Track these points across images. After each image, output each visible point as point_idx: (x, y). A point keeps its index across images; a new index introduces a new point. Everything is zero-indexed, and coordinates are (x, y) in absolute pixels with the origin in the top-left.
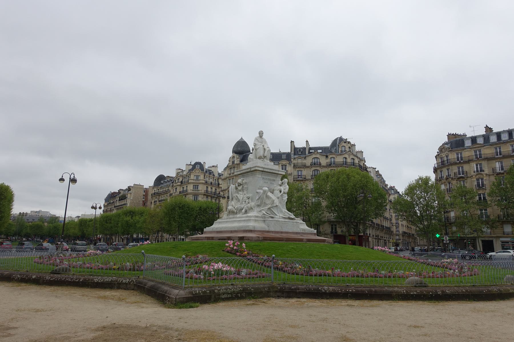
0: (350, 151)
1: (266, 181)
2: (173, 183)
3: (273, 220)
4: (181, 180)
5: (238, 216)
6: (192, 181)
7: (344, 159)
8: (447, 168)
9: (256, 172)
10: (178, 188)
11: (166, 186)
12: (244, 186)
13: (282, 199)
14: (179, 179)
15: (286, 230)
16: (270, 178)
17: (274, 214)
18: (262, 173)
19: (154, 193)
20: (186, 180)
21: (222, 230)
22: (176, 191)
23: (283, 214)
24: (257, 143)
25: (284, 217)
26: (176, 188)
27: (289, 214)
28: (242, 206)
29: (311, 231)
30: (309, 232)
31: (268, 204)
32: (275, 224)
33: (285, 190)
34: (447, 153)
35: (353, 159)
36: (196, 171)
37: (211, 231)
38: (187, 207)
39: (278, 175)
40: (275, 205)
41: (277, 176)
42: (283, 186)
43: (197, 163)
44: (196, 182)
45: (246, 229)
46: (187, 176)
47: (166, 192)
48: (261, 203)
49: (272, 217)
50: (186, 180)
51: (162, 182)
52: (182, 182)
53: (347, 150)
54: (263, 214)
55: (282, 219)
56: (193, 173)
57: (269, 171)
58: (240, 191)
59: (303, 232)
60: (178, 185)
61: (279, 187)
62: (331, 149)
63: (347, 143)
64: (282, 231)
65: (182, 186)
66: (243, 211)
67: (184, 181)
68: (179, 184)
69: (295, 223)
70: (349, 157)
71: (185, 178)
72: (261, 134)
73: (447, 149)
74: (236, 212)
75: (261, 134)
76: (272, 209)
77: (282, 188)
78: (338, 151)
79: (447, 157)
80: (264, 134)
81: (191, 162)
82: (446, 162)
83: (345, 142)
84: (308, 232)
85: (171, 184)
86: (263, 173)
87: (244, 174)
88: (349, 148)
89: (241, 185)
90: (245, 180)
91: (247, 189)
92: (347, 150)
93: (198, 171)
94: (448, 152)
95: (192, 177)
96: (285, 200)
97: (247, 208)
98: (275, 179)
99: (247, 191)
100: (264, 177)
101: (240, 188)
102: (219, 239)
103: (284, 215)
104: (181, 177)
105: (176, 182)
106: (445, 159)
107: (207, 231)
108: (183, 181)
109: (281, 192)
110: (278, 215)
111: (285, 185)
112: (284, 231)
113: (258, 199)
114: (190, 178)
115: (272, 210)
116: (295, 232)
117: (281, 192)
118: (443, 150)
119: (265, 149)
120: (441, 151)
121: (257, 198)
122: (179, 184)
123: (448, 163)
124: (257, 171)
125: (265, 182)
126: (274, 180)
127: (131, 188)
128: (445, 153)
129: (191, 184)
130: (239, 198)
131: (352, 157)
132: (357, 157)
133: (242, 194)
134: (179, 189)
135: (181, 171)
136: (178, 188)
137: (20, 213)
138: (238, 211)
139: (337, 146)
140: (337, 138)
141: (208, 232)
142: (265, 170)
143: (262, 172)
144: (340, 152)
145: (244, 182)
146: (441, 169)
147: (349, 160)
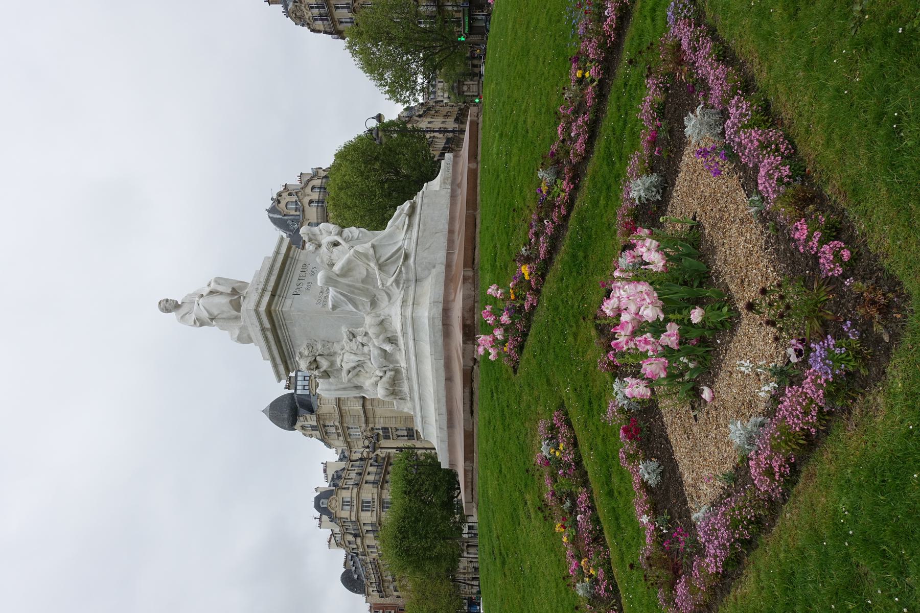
0: (296, 193)
2: (357, 554)
4: (350, 538)
5: (403, 364)
6: (354, 514)
7: (311, 204)
8: (334, 10)
9: (274, 315)
10: (368, 542)
11: (364, 568)
12: (320, 352)
13: (357, 239)
14: (349, 541)
16: (295, 280)
17: (397, 255)
19: (378, 592)
20: (351, 527)
21: (444, 410)
22: (373, 547)
23: (398, 231)
24: (193, 317)
26: (368, 546)
27: (400, 215)
28: (375, 352)
30: (451, 168)
31: (367, 270)
32: (428, 248)
33: (331, 233)
34: (305, 7)
35: (313, 188)
36: (333, 505)
37: (449, 446)
38: (404, 522)
39: (291, 255)
40: (371, 251)
41: (292, 258)
42: (320, 237)
43: (317, 506)
44: (355, 506)
45: (441, 327)
46: (342, 526)
47: (376, 567)
48: (365, 292)
49: (407, 257)
50: (351, 527)
51: (356, 577)
52: (356, 536)
53: (294, 198)
54: (398, 286)
56: (338, 512)
57: (273, 278)
58: (332, 364)
59: (450, 181)
60: (362, 543)
61: (324, 249)
62: (292, 231)
63: (279, 198)
64: (446, 232)
65: (365, 535)
66: (388, 347)
67: (354, 530)
68: (359, 541)
69: (425, 201)
70: (309, 195)
71: (347, 529)
72: (169, 306)
73: (296, 6)
74: (392, 373)
75: (169, 306)
76: (382, 260)
77: (326, 240)
78: (297, 217)
79: (312, 8)
80: (169, 299)
81: (316, 518)
82: (322, 10)
83: (279, 202)
84: (451, 171)
85: (360, 557)
86: (278, 292)
87: (285, 356)
88: (290, 194)
89: (315, 360)
90: (302, 349)
91: (328, 342)
92: (294, 198)
93: (333, 502)
94: (303, 5)
95: (345, 514)
96: (361, 232)
97: (380, 335)
98: (300, 265)
99: (333, 343)
100: (291, 291)
101: (324, 364)
102: (472, 412)
103: (401, 227)
104: (345, 537)
105: (355, 546)
106: (316, 11)
107: (448, 460)
108: (353, 532)
109: (336, 244)
110: (400, 244)
111: (318, 232)
113: (355, 305)
114: (347, 519)
116: (449, 201)
117: (336, 244)
118: (297, 14)
119: (211, 293)
120: (300, 18)
121: (350, 307)
122: (359, 541)
123: (324, 8)
124: (273, 308)
125: (308, 289)
126: (305, 266)
128: (304, 10)
129: (359, 515)
130: (353, 364)
131: (308, 190)
132: (309, 181)
133: (341, 357)
134: (370, 540)
135: (333, 538)
136: (368, 542)
138: (391, 366)
139: (286, 218)
140: (269, 217)
141: (450, 457)
142: (270, 288)
143: (277, 297)
144: (298, 213)
145: (306, 353)
146: (335, 21)
147: (315, 196)
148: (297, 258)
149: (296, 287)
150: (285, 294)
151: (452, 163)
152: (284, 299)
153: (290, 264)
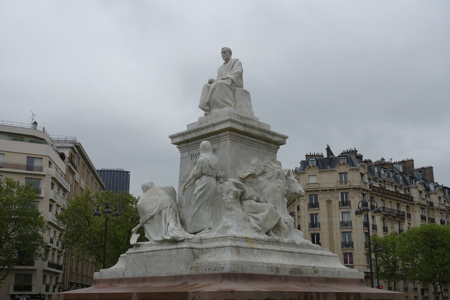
18: (188, 148)
30: (210, 272)
32: (134, 263)
39: (219, 135)
41: (218, 137)
59: (194, 272)
64: (146, 275)
69: (174, 252)
84: (207, 272)
112: (150, 275)
142: (186, 138)
143: (185, 145)
148: (221, 140)
151: (216, 272)
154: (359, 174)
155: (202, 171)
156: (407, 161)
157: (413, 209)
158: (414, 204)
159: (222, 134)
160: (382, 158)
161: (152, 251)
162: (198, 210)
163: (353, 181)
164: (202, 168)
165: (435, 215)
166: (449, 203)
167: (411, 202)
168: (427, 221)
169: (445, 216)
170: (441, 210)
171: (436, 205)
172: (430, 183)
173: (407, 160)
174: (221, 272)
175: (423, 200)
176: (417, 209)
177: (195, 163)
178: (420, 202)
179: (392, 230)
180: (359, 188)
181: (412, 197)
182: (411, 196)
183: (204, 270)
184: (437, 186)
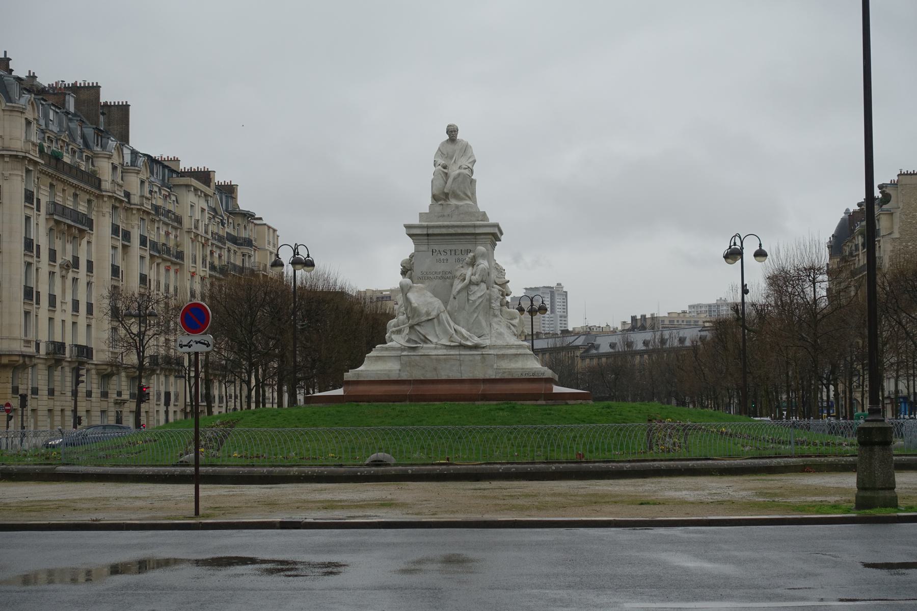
1: (442, 257)
3: (415, 354)
15: (450, 375)
16: (453, 247)
25: (448, 344)
29: (534, 374)
39: (478, 237)
41: (476, 239)
55: (441, 351)
72: (452, 132)
75: (452, 132)
84: (523, 377)
100: (436, 247)
110: (434, 340)
112: (444, 378)
115: (418, 331)
127: (888, 191)
137: (634, 319)
142: (430, 231)
143: (426, 238)
149: (442, 250)
150: (432, 243)
152: (427, 243)
153: (469, 239)
154: (24, 121)
155: (482, 279)
156: (85, 87)
157: (98, 207)
158: (103, 196)
159: (482, 237)
160: (30, 71)
161: (444, 355)
162: (477, 316)
163: (10, 139)
164: (483, 276)
165: (131, 222)
166: (151, 195)
167: (97, 192)
168: (120, 238)
169: (148, 225)
170: (144, 211)
171: (135, 199)
172: (126, 145)
173: (85, 84)
174: (541, 377)
175: (119, 189)
176: (107, 208)
177: (438, 260)
178: (115, 193)
179: (64, 257)
180: (25, 158)
181: (100, 180)
182: (98, 176)
183: (520, 375)
184: (134, 153)
